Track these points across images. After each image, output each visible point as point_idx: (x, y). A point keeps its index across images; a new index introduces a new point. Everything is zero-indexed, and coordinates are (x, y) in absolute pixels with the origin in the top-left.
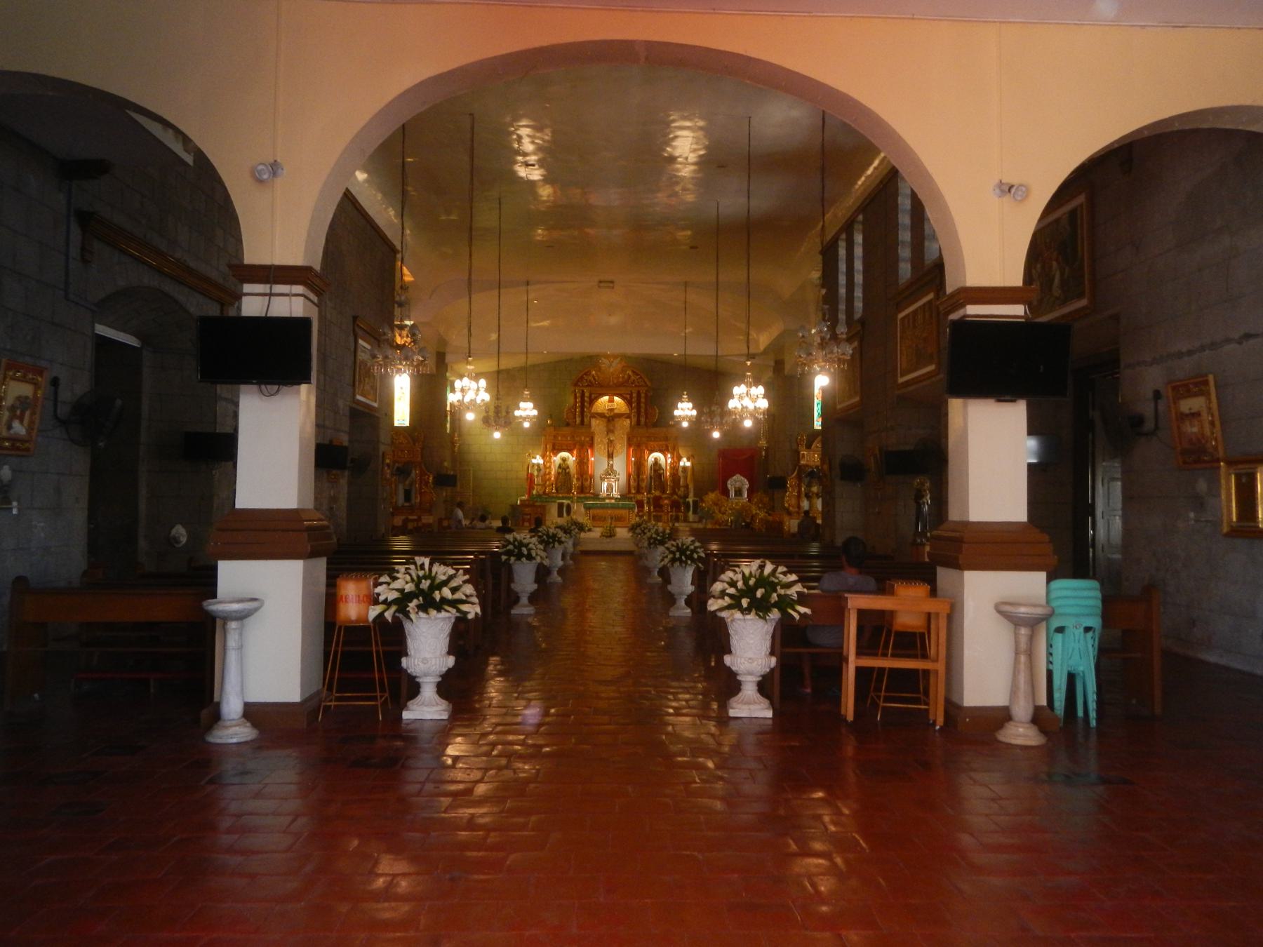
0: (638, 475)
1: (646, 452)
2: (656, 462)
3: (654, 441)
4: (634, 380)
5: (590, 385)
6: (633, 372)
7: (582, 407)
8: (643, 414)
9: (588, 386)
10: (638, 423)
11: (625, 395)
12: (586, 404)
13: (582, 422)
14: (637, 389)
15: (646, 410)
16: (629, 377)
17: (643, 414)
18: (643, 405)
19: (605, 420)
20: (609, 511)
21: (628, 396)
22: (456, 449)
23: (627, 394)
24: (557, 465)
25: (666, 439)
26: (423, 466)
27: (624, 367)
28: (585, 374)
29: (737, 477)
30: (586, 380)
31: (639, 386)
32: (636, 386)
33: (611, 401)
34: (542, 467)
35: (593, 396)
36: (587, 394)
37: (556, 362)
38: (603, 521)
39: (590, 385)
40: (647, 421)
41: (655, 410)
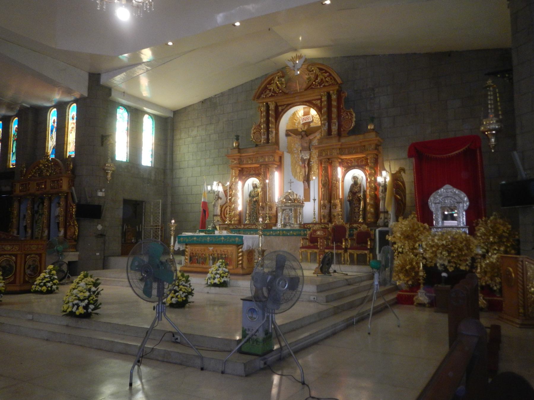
0: (330, 202)
1: (340, 170)
2: (356, 182)
3: (350, 153)
4: (322, 80)
5: (275, 94)
6: (321, 69)
7: (268, 122)
8: (335, 121)
9: (272, 96)
10: (329, 132)
11: (314, 102)
12: (270, 118)
13: (268, 139)
14: (326, 89)
15: (339, 116)
16: (317, 77)
17: (335, 121)
18: (334, 110)
19: (300, 137)
20: (211, 249)
21: (319, 102)
22: (109, 176)
23: (318, 100)
24: (247, 193)
25: (363, 149)
26: (70, 195)
27: (309, 65)
28: (269, 83)
29: (447, 190)
30: (270, 90)
31: (330, 85)
32: (324, 86)
33: (306, 114)
34: (222, 194)
35: (280, 108)
36: (272, 107)
37: (252, 81)
38: (203, 263)
39: (275, 94)
40: (342, 130)
41: (351, 114)
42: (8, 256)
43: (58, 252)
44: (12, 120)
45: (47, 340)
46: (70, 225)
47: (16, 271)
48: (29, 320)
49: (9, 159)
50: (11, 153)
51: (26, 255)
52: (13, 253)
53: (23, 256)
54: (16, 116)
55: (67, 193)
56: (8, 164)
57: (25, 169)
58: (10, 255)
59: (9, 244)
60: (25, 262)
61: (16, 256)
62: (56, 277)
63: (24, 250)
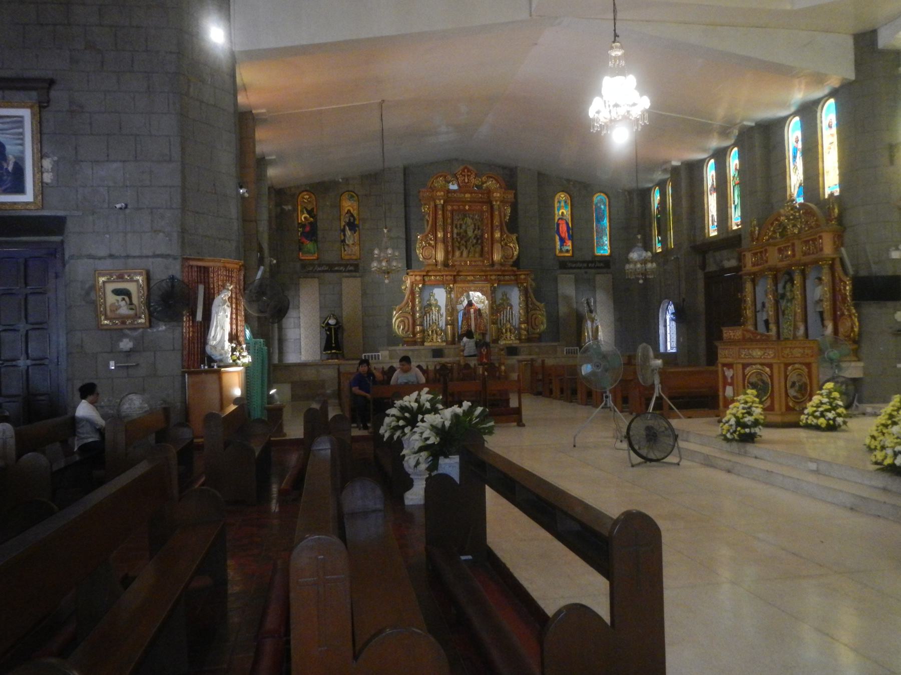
42: (759, 367)
43: (831, 360)
44: (728, 153)
45: (852, 509)
46: (843, 314)
47: (772, 391)
48: (812, 471)
49: (729, 216)
50: (733, 206)
51: (787, 365)
52: (766, 361)
53: (782, 366)
54: (735, 145)
55: (833, 260)
56: (729, 224)
57: (757, 228)
58: (762, 364)
59: (759, 348)
60: (786, 377)
61: (770, 366)
62: (840, 403)
63: (783, 357)
